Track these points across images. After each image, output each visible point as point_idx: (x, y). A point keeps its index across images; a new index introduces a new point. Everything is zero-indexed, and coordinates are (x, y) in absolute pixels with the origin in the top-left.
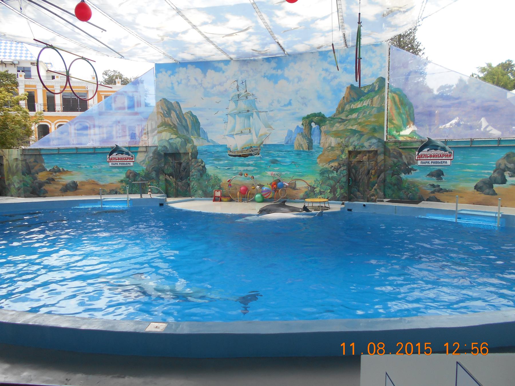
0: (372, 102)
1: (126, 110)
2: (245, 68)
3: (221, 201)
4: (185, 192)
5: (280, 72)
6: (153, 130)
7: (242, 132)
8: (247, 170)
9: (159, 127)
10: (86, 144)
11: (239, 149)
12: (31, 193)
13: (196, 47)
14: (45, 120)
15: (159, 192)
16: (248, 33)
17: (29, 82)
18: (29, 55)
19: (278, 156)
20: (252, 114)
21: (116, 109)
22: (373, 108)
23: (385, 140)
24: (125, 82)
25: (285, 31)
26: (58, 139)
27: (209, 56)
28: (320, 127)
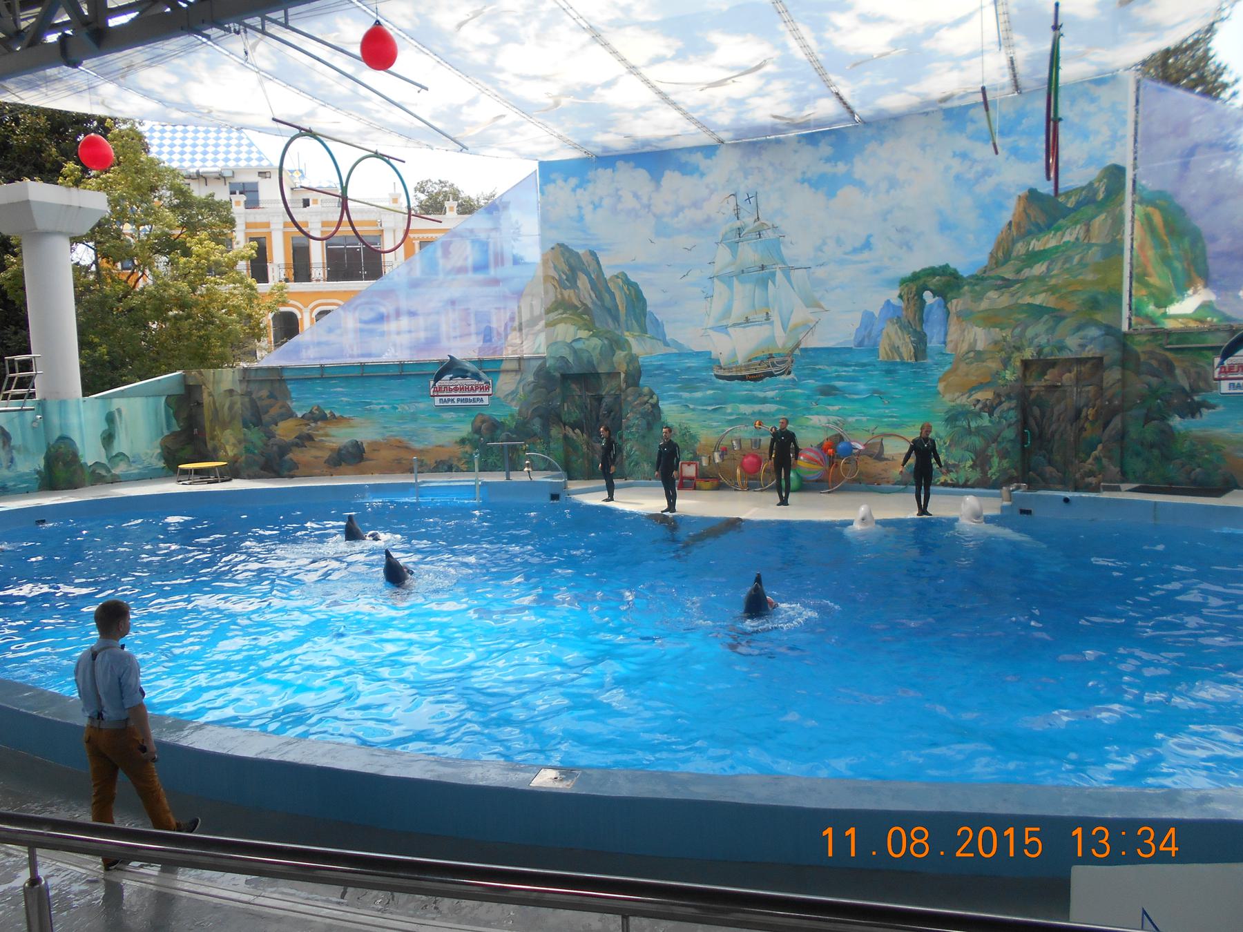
0: (1088, 231)
1: (471, 275)
2: (754, 162)
3: (695, 488)
4: (609, 469)
5: (841, 168)
6: (533, 321)
7: (747, 320)
8: (760, 413)
9: (548, 311)
10: (380, 356)
11: (741, 361)
12: (263, 468)
13: (637, 117)
14: (291, 302)
15: (549, 467)
16: (762, 76)
17: (256, 216)
18: (254, 156)
19: (839, 378)
20: (773, 274)
21: (448, 273)
22: (1090, 246)
23: (1125, 328)
24: (467, 208)
25: (855, 65)
26: (319, 344)
27: (668, 138)
28: (946, 303)
